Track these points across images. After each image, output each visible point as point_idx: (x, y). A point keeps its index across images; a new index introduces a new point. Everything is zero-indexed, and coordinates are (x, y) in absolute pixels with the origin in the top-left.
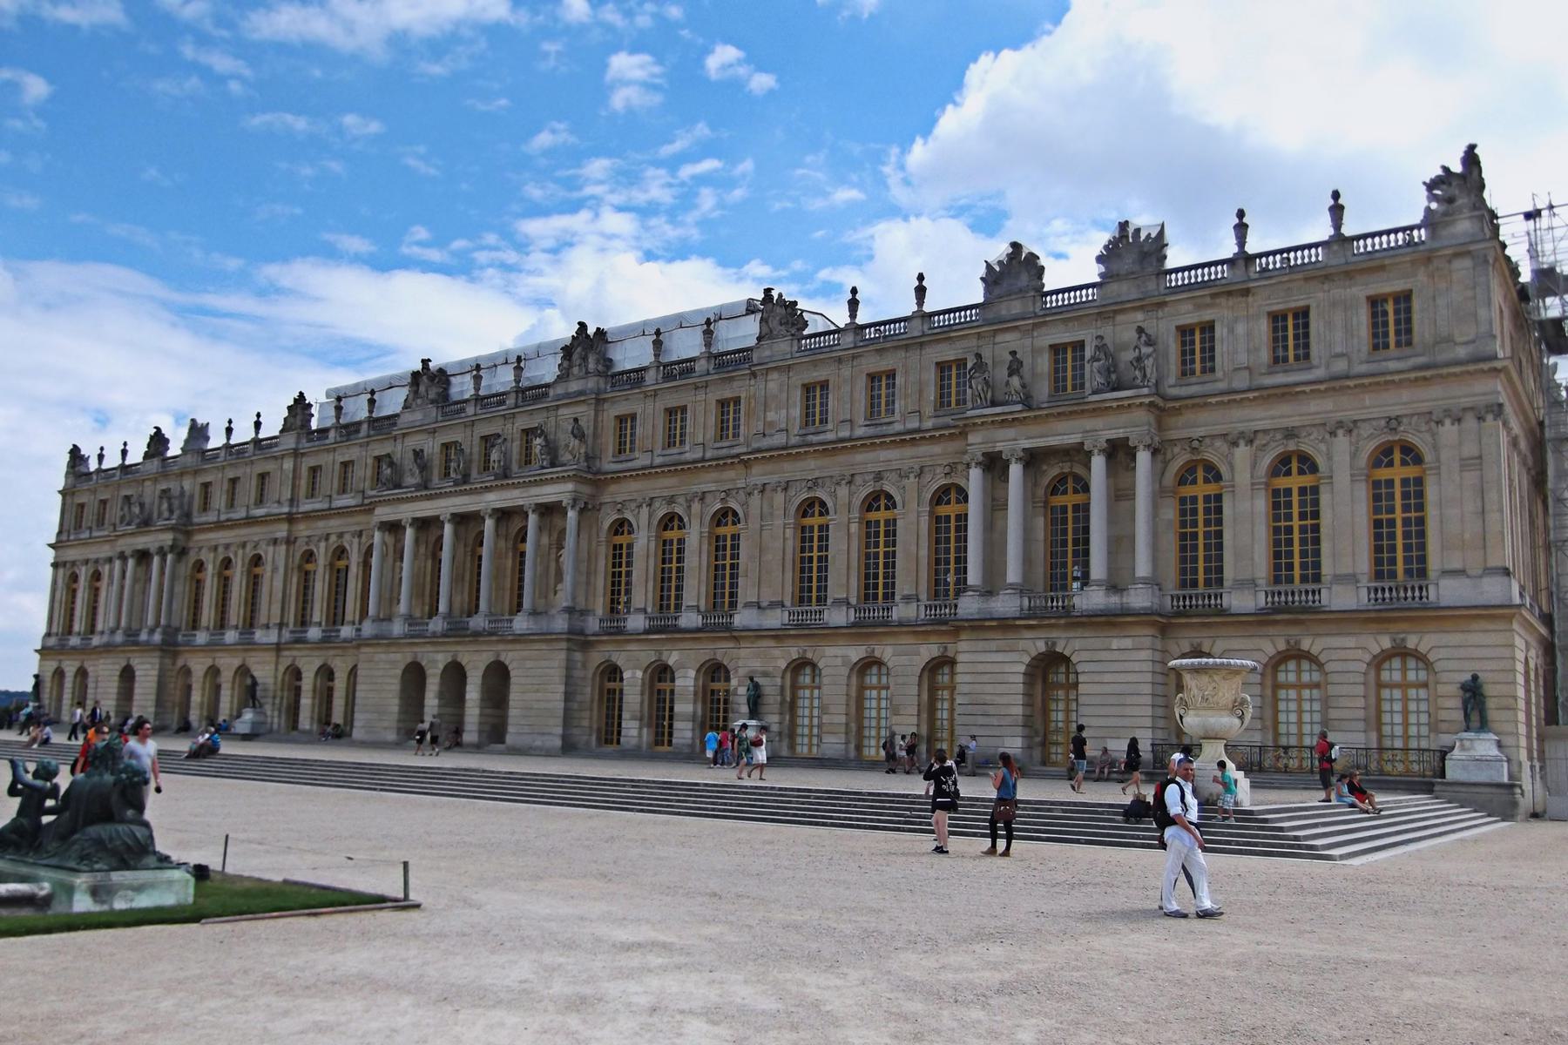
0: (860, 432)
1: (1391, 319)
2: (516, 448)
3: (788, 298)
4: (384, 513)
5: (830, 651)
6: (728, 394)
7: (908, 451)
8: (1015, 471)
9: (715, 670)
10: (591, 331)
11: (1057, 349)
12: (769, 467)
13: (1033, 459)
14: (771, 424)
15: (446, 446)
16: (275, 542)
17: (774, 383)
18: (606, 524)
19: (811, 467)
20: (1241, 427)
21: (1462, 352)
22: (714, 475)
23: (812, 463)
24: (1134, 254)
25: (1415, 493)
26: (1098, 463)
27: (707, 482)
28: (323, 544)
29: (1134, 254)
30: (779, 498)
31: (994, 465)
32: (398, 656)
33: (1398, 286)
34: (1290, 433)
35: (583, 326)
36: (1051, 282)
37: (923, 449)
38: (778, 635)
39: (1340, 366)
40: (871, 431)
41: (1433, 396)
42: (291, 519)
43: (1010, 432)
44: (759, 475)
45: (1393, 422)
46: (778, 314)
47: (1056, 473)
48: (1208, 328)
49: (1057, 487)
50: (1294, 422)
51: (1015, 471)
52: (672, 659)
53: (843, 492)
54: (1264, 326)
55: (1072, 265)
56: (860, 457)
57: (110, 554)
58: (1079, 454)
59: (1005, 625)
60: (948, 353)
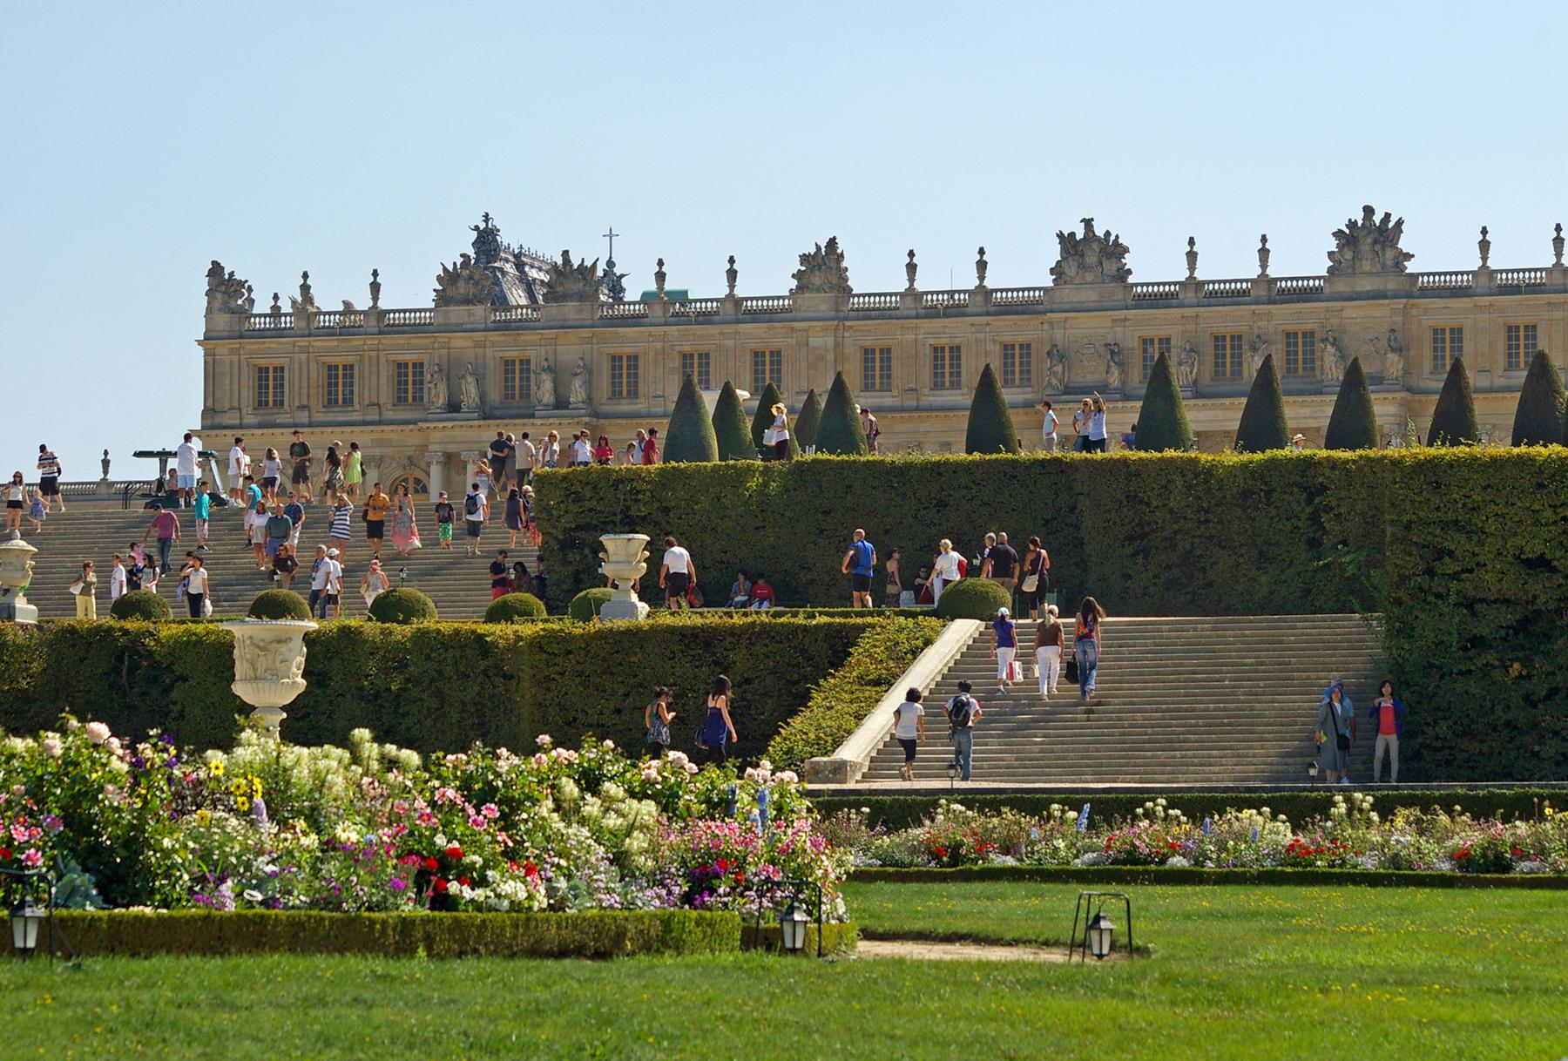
10: (1377, 219)
35: (1369, 211)
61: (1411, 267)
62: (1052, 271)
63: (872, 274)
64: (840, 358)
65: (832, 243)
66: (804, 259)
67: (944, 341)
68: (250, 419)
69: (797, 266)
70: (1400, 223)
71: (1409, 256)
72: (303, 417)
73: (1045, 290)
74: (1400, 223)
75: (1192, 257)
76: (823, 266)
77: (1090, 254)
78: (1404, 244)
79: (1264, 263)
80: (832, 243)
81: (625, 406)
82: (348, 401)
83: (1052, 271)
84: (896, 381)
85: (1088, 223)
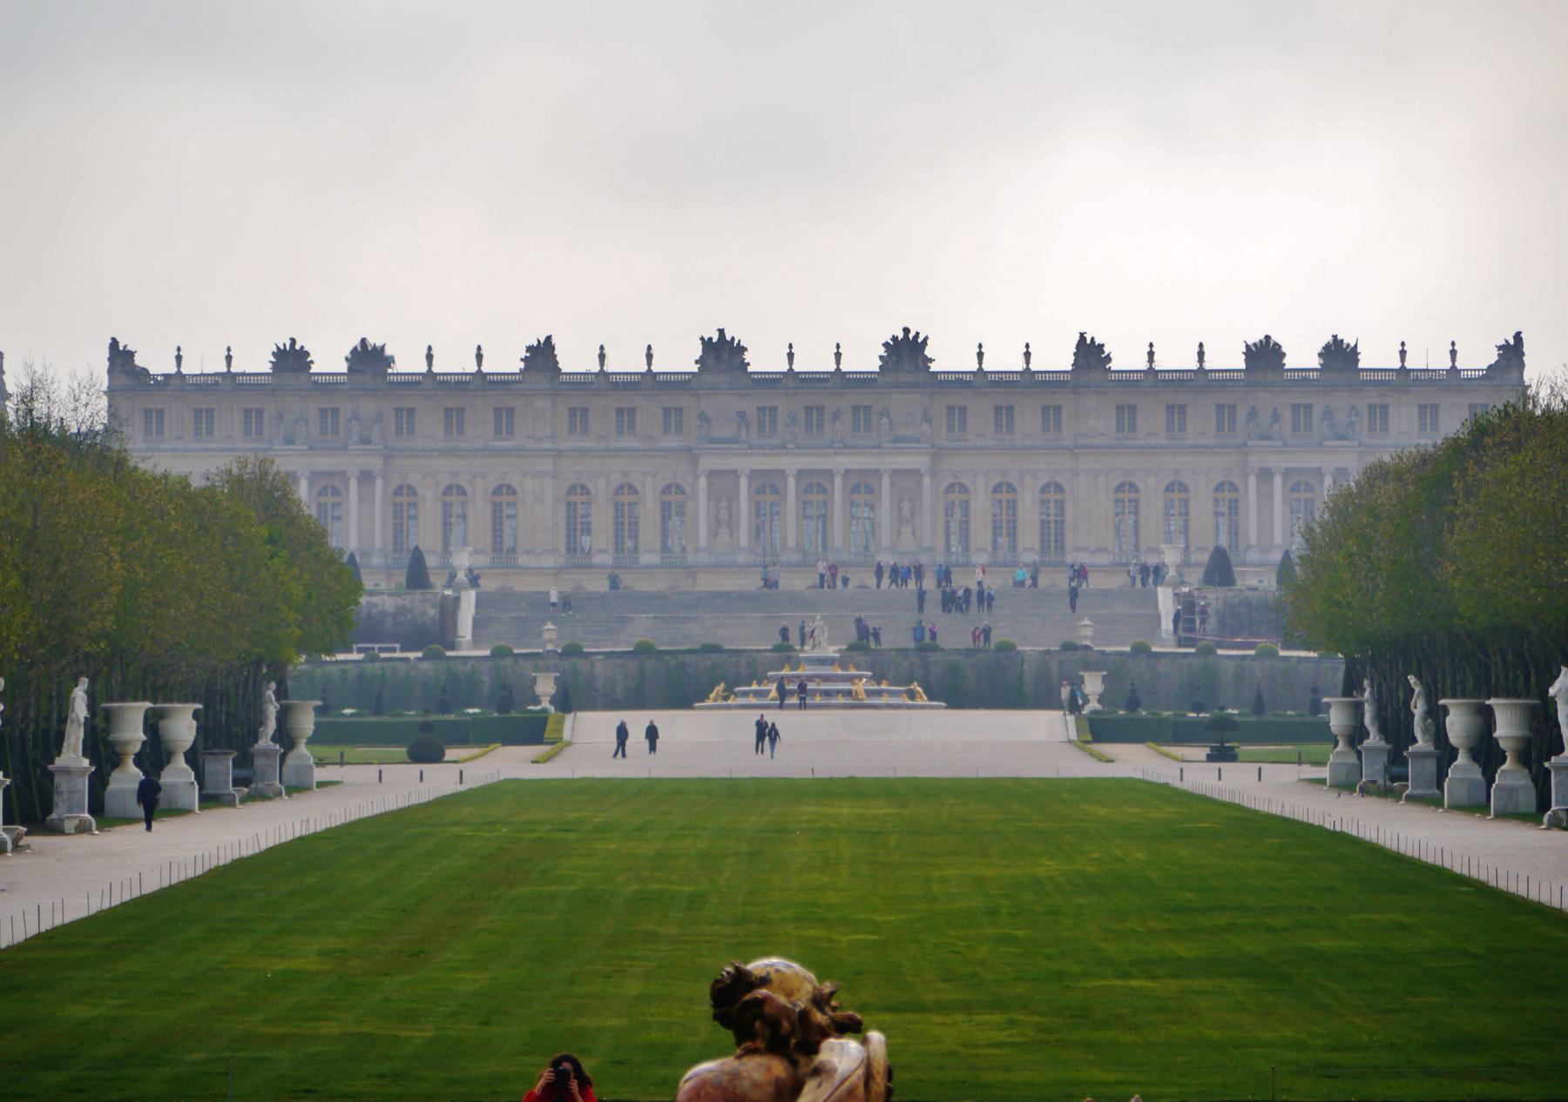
0: (1161, 442)
2: (847, 418)
4: (708, 463)
8: (1278, 480)
11: (1295, 407)
13: (1287, 473)
15: (761, 409)
18: (944, 485)
28: (602, 482)
29: (1339, 354)
31: (1265, 475)
35: (906, 331)
36: (1290, 362)
42: (560, 454)
46: (1089, 353)
48: (1385, 408)
49: (1295, 488)
51: (1278, 480)
54: (1416, 411)
61: (934, 367)
63: (574, 359)
65: (549, 338)
66: (529, 349)
67: (624, 404)
69: (524, 354)
70: (926, 339)
71: (931, 360)
73: (693, 374)
74: (926, 339)
75: (791, 356)
76: (542, 354)
78: (928, 352)
79: (838, 362)
80: (549, 338)
85: (721, 332)
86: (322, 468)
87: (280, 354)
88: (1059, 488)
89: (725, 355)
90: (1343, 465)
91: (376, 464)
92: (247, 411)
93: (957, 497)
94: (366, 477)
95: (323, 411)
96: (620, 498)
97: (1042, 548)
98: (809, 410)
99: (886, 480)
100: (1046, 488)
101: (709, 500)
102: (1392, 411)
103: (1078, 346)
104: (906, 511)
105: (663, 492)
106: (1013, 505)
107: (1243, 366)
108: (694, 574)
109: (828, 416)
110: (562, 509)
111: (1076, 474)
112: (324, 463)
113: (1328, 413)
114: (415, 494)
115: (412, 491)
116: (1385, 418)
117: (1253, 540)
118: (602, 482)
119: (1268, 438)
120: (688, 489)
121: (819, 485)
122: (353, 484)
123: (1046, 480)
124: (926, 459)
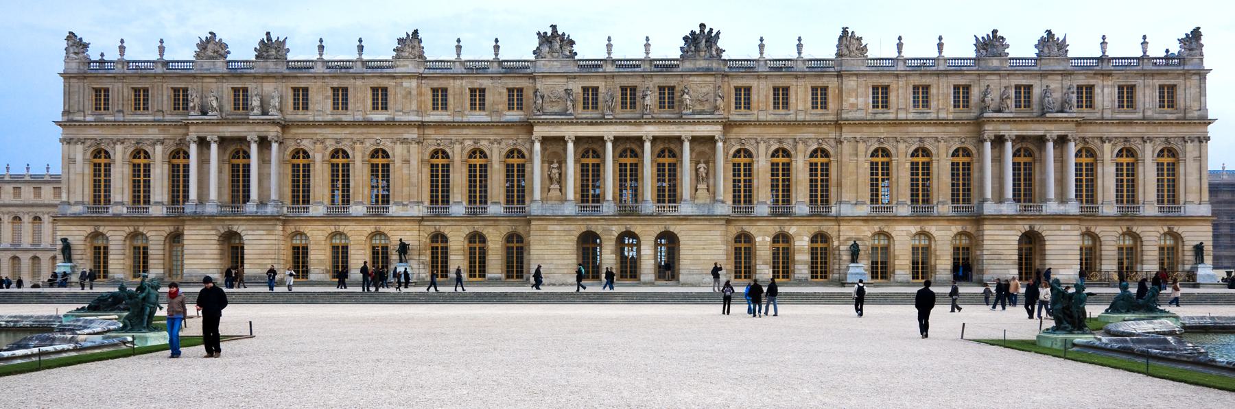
0: (910, 116)
1: (1168, 96)
3: (857, 35)
4: (539, 132)
5: (899, 228)
6: (820, 83)
7: (941, 129)
8: (1009, 145)
9: (820, 238)
10: (706, 31)
12: (854, 129)
14: (852, 105)
15: (585, 89)
16: (404, 141)
17: (850, 83)
18: (732, 152)
19: (882, 132)
20: (1106, 135)
21: (1196, 114)
22: (813, 129)
23: (882, 130)
24: (1050, 44)
25: (1173, 168)
26: (1050, 145)
27: (808, 133)
28: (458, 147)
29: (1050, 44)
30: (861, 147)
31: (999, 141)
32: (572, 227)
33: (1172, 82)
34: (1126, 140)
35: (702, 26)
36: (1012, 52)
37: (949, 129)
38: (866, 220)
39: (1149, 113)
40: (917, 116)
41: (1184, 131)
42: (422, 125)
43: (1008, 127)
44: (847, 133)
45: (1167, 139)
47: (1030, 148)
48: (1090, 88)
50: (1130, 135)
51: (1009, 145)
52: (792, 230)
53: (902, 146)
55: (1022, 46)
56: (911, 129)
57: (161, 137)
58: (1041, 140)
59: (1010, 219)
60: (961, 81)
61: (724, 56)
62: (534, 52)
64: (420, 94)
65: (416, 32)
66: (400, 41)
67: (476, 85)
68: (89, 118)
69: (395, 45)
70: (718, 33)
72: (120, 117)
74: (718, 33)
77: (554, 41)
78: (721, 44)
80: (416, 32)
81: (301, 116)
82: (146, 109)
83: (534, 52)
84: (451, 106)
85: (554, 27)
86: (228, 135)
87: (203, 46)
88: (825, 153)
89: (557, 46)
90: (1062, 133)
91: (272, 132)
92: (176, 90)
93: (742, 160)
94: (264, 143)
95: (236, 90)
96: (473, 161)
97: (811, 201)
98: (623, 89)
99: (687, 145)
100: (814, 154)
101: (543, 162)
102: (1097, 90)
103: (841, 38)
104: (702, 171)
105: (508, 156)
106: (787, 168)
107: (973, 55)
108: (529, 222)
109: (639, 94)
110: (426, 171)
111: (839, 142)
112: (229, 131)
113: (1046, 92)
114: (308, 157)
115: (306, 155)
116: (1090, 98)
117: (989, 195)
118: (458, 147)
119: (1000, 111)
120: (527, 154)
121: (632, 151)
122: (254, 149)
123: (815, 146)
124: (720, 128)
